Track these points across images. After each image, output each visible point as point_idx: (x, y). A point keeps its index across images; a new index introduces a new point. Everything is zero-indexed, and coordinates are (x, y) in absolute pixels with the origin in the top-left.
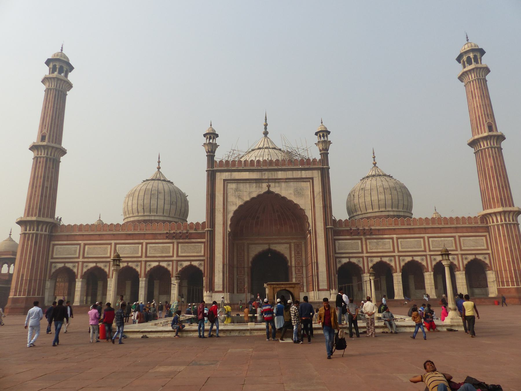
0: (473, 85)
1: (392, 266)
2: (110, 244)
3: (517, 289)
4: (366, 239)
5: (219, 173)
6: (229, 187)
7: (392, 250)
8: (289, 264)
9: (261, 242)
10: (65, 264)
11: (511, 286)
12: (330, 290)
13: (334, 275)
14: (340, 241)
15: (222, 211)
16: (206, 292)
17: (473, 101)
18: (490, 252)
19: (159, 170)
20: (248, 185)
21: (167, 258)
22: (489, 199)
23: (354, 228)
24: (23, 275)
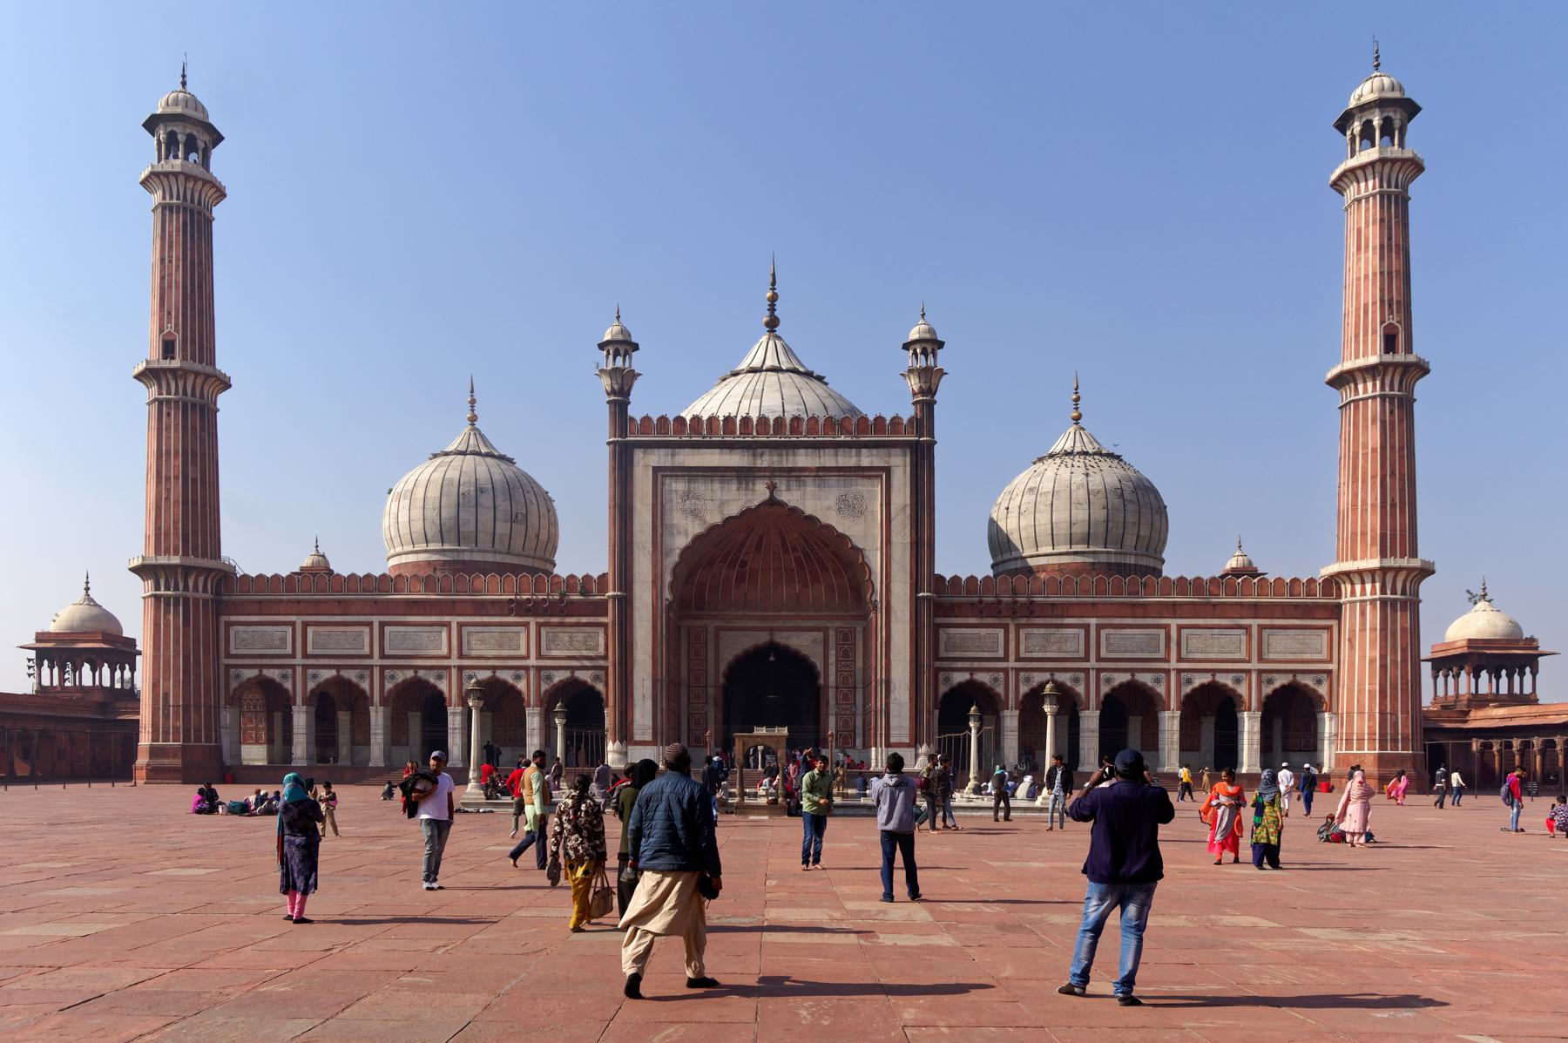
1: (1078, 694)
2: (370, 624)
3: (1380, 756)
4: (1018, 627)
6: (667, 487)
7: (1082, 655)
9: (751, 624)
13: (928, 711)
14: (952, 631)
15: (651, 548)
23: (989, 599)
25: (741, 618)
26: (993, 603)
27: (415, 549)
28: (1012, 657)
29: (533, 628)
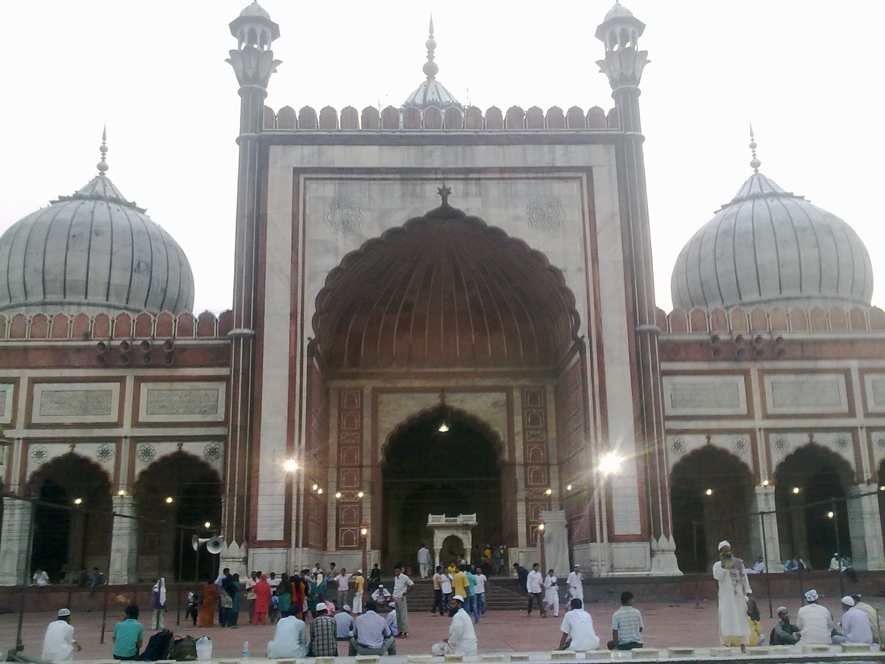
1: (846, 464)
4: (763, 372)
5: (280, 147)
7: (845, 408)
8: (506, 456)
9: (417, 384)
12: (650, 536)
14: (678, 379)
16: (228, 546)
19: (102, 174)
20: (375, 187)
21: (102, 430)
25: (405, 376)
26: (727, 343)
27: (11, 304)
28: (758, 413)
29: (130, 383)
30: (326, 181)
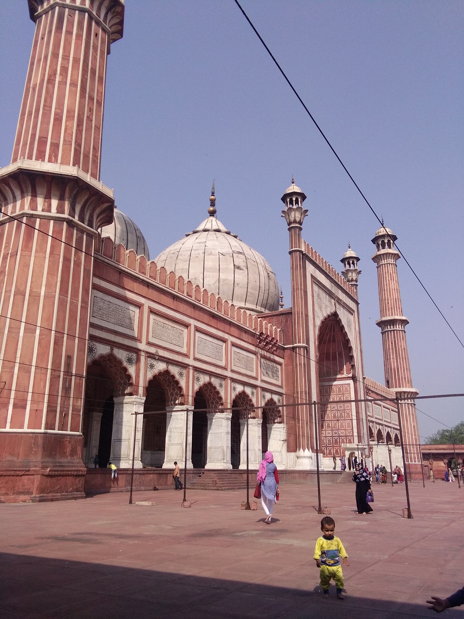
0: (392, 268)
10: (112, 349)
11: (417, 462)
17: (392, 283)
18: (399, 428)
22: (402, 378)
24: (69, 358)
30: (316, 285)
